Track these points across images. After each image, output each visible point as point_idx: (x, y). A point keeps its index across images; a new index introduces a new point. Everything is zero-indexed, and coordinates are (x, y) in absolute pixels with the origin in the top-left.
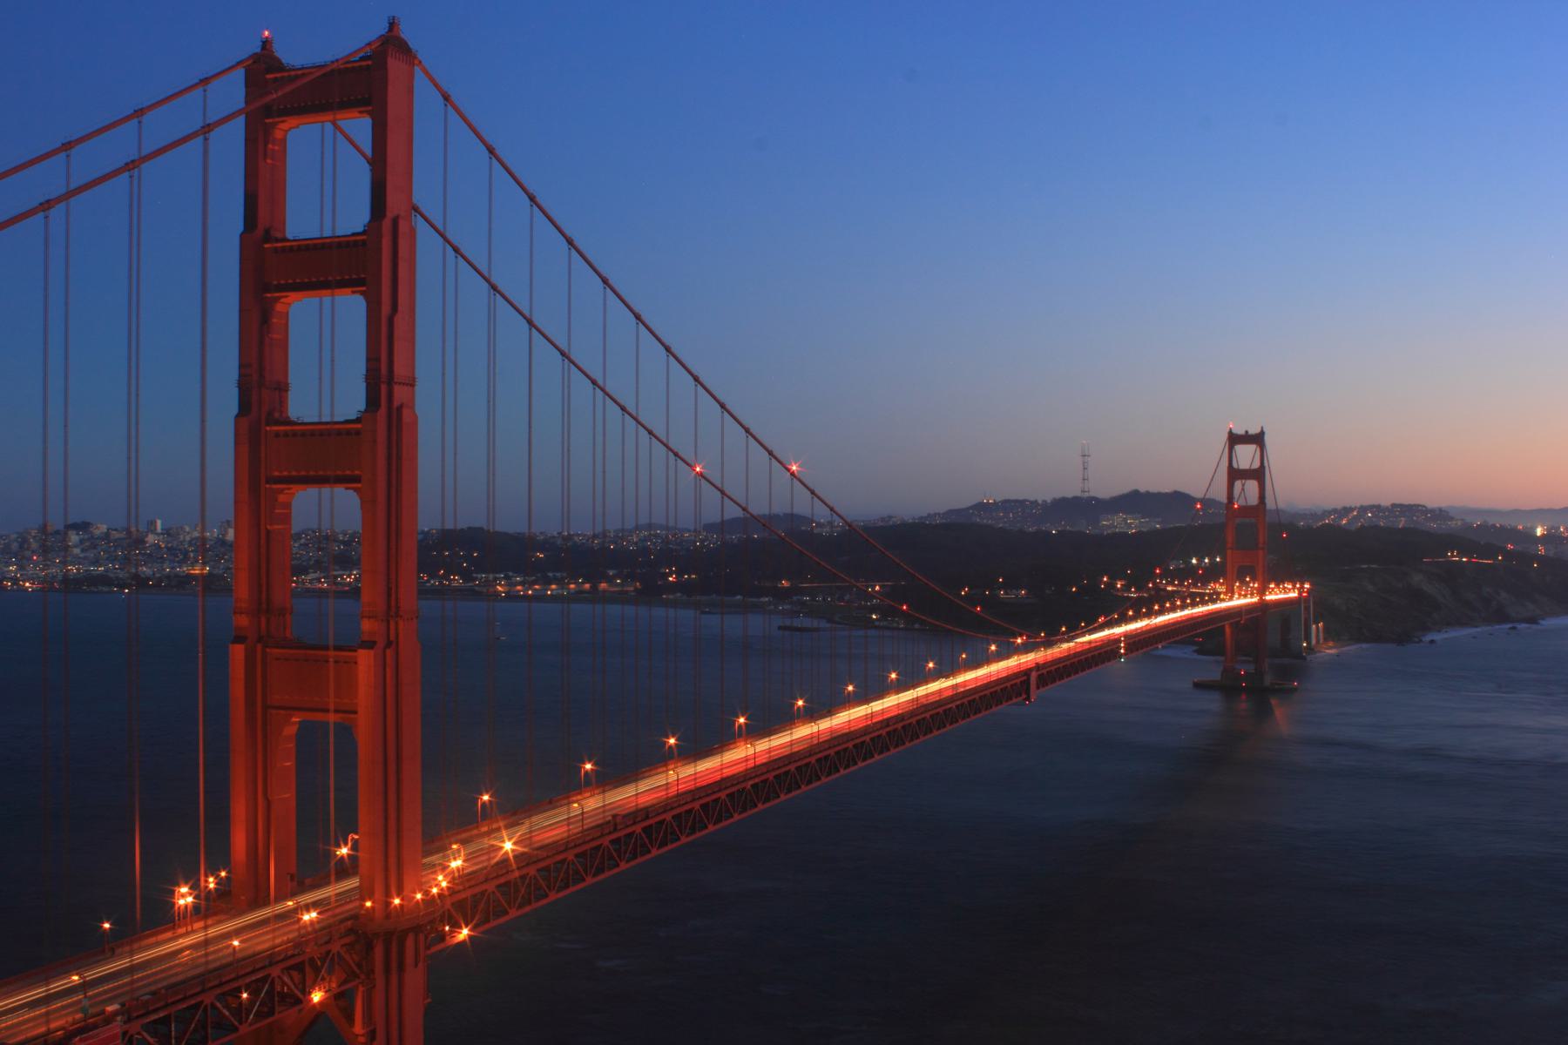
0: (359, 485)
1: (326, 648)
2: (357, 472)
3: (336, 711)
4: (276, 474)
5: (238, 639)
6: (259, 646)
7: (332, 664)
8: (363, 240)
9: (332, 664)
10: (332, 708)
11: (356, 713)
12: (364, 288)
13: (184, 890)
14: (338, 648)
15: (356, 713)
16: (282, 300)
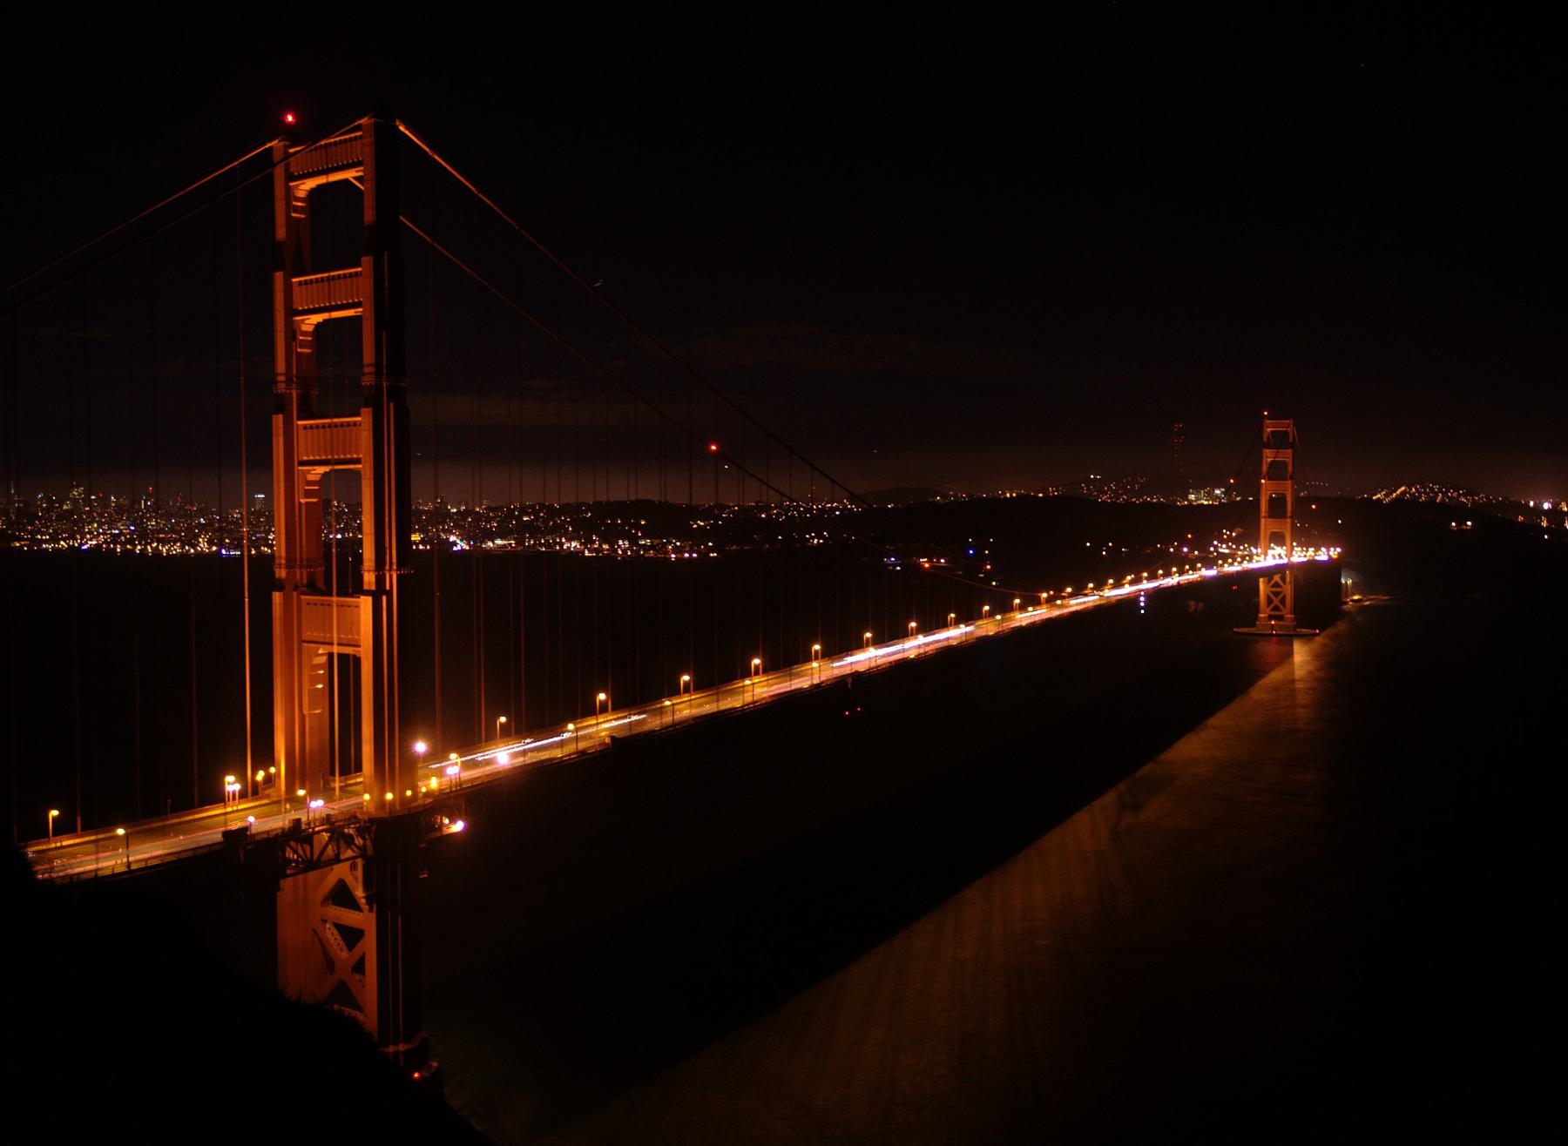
0: (360, 466)
1: (331, 595)
2: (361, 456)
3: (339, 644)
4: (305, 458)
5: (280, 588)
6: (295, 593)
7: (335, 609)
8: (361, 272)
9: (335, 609)
10: (335, 641)
11: (359, 646)
12: (361, 310)
13: (230, 779)
14: (339, 595)
15: (359, 646)
16: (307, 322)
